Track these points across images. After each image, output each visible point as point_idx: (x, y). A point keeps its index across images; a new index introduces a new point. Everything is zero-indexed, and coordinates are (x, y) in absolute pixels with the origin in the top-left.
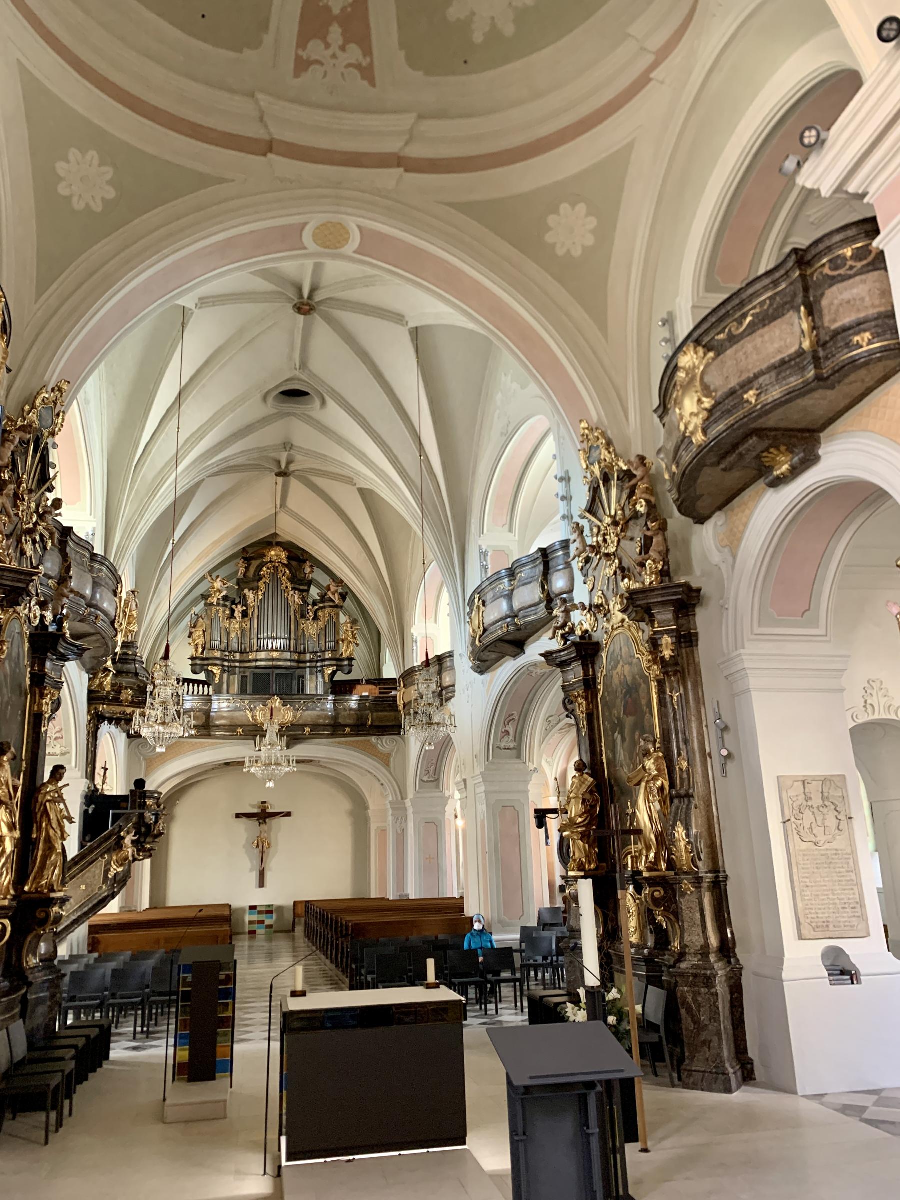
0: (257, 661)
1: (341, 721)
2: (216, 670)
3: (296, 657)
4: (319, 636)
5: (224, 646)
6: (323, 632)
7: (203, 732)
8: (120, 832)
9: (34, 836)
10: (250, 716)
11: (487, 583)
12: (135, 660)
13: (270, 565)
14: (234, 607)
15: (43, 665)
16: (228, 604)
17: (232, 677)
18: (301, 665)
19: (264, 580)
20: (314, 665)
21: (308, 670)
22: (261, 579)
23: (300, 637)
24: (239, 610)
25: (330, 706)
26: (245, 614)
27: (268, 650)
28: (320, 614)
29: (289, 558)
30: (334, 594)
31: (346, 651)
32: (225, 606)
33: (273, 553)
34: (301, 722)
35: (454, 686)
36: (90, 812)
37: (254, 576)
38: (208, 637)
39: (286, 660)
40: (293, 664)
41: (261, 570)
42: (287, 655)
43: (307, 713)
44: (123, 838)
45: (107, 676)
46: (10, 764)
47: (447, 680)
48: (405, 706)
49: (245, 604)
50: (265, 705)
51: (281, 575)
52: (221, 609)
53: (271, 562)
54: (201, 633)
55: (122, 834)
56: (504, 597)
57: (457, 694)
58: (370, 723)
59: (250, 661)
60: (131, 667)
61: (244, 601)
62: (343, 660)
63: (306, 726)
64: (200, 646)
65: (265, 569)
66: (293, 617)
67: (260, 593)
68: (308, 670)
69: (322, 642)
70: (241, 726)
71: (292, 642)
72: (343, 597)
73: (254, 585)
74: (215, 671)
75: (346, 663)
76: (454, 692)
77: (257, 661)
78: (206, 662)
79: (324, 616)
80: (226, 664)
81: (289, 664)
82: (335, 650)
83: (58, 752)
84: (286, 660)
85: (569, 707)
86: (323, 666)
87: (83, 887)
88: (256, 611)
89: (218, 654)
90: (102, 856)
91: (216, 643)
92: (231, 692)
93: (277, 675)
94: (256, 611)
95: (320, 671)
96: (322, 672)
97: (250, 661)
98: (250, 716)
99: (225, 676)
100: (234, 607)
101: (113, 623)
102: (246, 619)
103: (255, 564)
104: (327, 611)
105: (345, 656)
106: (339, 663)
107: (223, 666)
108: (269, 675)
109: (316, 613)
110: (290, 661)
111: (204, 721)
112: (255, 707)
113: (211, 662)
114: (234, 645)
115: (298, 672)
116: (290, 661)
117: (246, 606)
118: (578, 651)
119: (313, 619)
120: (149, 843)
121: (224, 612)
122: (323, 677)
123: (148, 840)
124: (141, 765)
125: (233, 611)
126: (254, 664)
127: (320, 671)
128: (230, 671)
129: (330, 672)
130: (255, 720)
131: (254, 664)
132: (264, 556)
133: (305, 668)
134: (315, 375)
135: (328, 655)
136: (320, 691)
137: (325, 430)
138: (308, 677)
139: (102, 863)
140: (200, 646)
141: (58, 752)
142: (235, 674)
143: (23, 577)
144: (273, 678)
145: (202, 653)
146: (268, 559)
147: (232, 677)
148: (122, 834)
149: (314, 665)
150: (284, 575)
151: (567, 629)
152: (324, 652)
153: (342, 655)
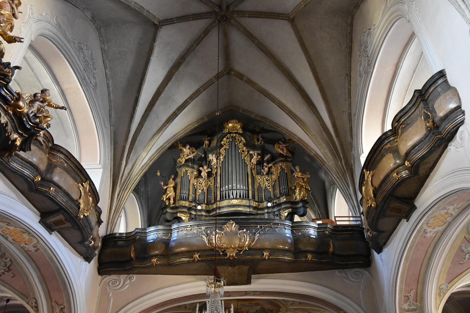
0: (220, 208)
1: (302, 247)
3: (254, 204)
4: (274, 187)
5: (190, 198)
6: (277, 183)
7: (164, 261)
13: (229, 135)
14: (201, 168)
18: (259, 212)
19: (224, 147)
20: (270, 210)
22: (221, 146)
25: (288, 233)
26: (209, 174)
28: (273, 170)
29: (243, 128)
31: (300, 194)
32: (193, 168)
33: (230, 125)
34: (258, 246)
38: (178, 191)
40: (251, 210)
41: (222, 140)
42: (245, 202)
49: (209, 166)
50: (221, 229)
51: (238, 142)
52: (190, 170)
53: (230, 133)
54: (172, 189)
58: (331, 250)
59: (214, 210)
62: (297, 203)
64: (172, 199)
66: (249, 173)
67: (221, 157)
69: (277, 191)
70: (198, 251)
74: (184, 218)
75: (300, 205)
77: (220, 208)
78: (175, 211)
80: (193, 213)
81: (248, 210)
86: (279, 210)
88: (219, 170)
89: (186, 204)
94: (219, 170)
100: (201, 168)
102: (211, 178)
106: (294, 206)
107: (191, 214)
109: (270, 168)
110: (249, 207)
111: (163, 249)
112: (212, 232)
113: (180, 210)
117: (212, 169)
119: (267, 174)
124: (109, 300)
125: (200, 172)
127: (277, 215)
129: (286, 214)
130: (211, 244)
135: (283, 199)
140: (172, 199)
146: (226, 131)
149: (270, 210)
150: (240, 142)
153: (296, 199)
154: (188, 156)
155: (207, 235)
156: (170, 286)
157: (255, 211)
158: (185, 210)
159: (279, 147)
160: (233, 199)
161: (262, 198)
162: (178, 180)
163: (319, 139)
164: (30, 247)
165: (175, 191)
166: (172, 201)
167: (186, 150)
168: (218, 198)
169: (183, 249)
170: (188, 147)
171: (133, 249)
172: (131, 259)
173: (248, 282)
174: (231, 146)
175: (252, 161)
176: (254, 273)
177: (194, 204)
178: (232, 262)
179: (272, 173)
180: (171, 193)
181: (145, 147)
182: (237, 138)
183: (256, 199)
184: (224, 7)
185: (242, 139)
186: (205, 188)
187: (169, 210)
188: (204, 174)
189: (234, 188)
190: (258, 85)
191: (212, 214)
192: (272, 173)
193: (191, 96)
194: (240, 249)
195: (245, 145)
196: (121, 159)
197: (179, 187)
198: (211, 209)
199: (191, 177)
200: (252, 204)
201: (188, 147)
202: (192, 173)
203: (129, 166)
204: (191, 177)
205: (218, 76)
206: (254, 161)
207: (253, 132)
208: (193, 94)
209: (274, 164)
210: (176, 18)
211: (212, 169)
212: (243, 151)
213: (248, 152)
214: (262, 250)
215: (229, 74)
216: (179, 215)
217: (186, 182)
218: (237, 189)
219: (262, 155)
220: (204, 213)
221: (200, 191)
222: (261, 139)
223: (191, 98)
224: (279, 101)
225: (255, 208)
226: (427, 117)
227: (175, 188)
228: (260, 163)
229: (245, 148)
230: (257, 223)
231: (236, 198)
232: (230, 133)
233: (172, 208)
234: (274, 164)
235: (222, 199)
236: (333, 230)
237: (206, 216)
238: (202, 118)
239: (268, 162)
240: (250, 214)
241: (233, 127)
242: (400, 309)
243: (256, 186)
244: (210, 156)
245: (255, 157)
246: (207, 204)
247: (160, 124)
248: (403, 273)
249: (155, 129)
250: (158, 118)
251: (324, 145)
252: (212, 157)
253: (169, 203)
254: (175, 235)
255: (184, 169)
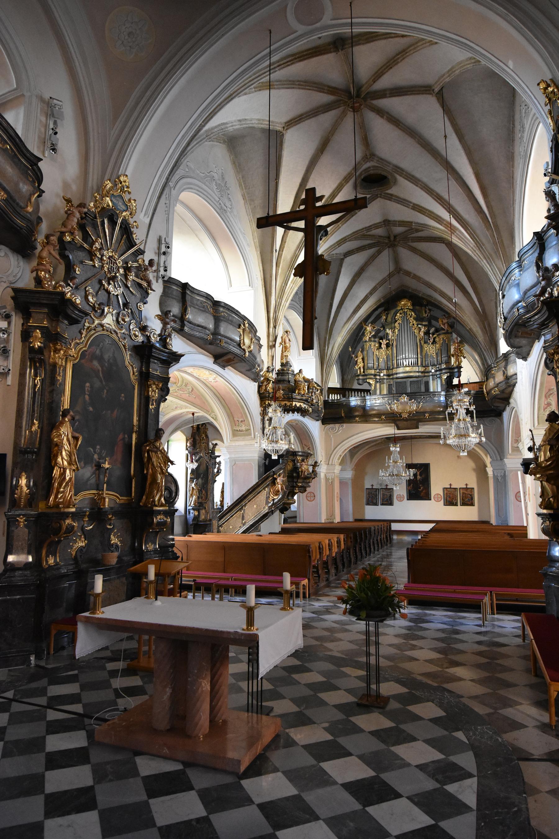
0: (397, 374)
2: (371, 382)
3: (421, 369)
4: (437, 354)
6: (439, 352)
8: (274, 475)
9: (145, 472)
10: (388, 408)
11: (504, 278)
12: (288, 373)
13: (401, 311)
14: (381, 341)
15: (148, 367)
16: (377, 340)
17: (382, 385)
18: (426, 374)
21: (431, 377)
22: (396, 321)
23: (425, 356)
24: (384, 342)
25: (442, 399)
26: (388, 345)
27: (403, 367)
28: (437, 339)
29: (413, 305)
30: (444, 324)
32: (375, 341)
33: (403, 303)
34: (422, 410)
35: (516, 374)
36: (267, 463)
37: (392, 319)
38: (366, 362)
39: (415, 372)
40: (420, 374)
42: (416, 369)
43: (425, 404)
44: (276, 479)
45: (269, 383)
46: (70, 423)
47: (511, 371)
48: (488, 395)
50: (398, 401)
51: (409, 317)
52: (373, 344)
53: (402, 309)
55: (275, 476)
56: (514, 286)
57: (518, 380)
59: (393, 375)
60: (286, 378)
61: (386, 336)
62: (454, 368)
63: (426, 412)
65: (398, 314)
66: (418, 344)
67: (396, 331)
68: (431, 377)
69: (439, 358)
70: (384, 414)
71: (419, 360)
72: (451, 326)
73: (393, 325)
74: (371, 382)
75: (456, 370)
76: (517, 379)
77: (397, 374)
78: (365, 377)
79: (440, 340)
80: (378, 377)
81: (417, 374)
82: (448, 362)
83: (244, 429)
84: (415, 372)
85: (550, 365)
86: (440, 374)
87: (255, 506)
89: (373, 372)
90: (264, 489)
91: (371, 365)
92: (382, 393)
93: (410, 381)
95: (439, 377)
96: (440, 377)
97: (393, 375)
98: (388, 408)
99: (378, 385)
100: (381, 341)
101: (239, 345)
102: (389, 348)
103: (393, 312)
104: (441, 337)
105: (455, 365)
106: (451, 371)
107: (376, 379)
108: (406, 382)
109: (434, 339)
110: (418, 372)
111: (362, 412)
113: (368, 377)
114: (382, 365)
115: (425, 379)
116: (418, 372)
117: (389, 340)
118: (549, 309)
119: (432, 343)
120: (300, 483)
121: (375, 345)
122: (441, 380)
123: (299, 481)
124: (331, 440)
125: (380, 344)
126: (395, 376)
128: (381, 381)
129: (445, 377)
131: (395, 376)
132: (396, 306)
133: (429, 376)
134: (381, 159)
135: (444, 366)
136: (439, 390)
137: (404, 202)
138: (431, 382)
139: (264, 493)
141: (244, 429)
142: (384, 383)
143: (54, 297)
144: (408, 384)
145: (364, 372)
147: (382, 385)
148: (275, 476)
150: (411, 317)
151: (547, 295)
152: (440, 364)
154: (371, 333)
155: (389, 404)
156: (367, 431)
157: (423, 375)
158: (372, 377)
159: (442, 321)
160: (406, 366)
161: (428, 364)
162: (365, 353)
163: (472, 319)
164: (294, 424)
165: (364, 362)
166: (362, 370)
167: (369, 329)
168: (395, 366)
169: (374, 412)
170: (370, 325)
171: (343, 412)
172: (342, 417)
173: (417, 428)
174: (403, 321)
175: (421, 333)
176: (421, 422)
177: (378, 371)
178: (406, 420)
179: (436, 343)
180: (361, 365)
181: (339, 334)
182: (408, 313)
183: (424, 365)
184: (392, 238)
185: (413, 313)
186: (385, 357)
187: (361, 377)
188: (384, 346)
189: (407, 357)
190: (423, 279)
191: (391, 377)
192: (436, 343)
193: (370, 292)
194: (410, 413)
195: (414, 319)
196: (325, 346)
197: (366, 358)
198: (391, 373)
199: (374, 349)
200: (420, 370)
201: (370, 325)
202: (375, 345)
203: (330, 349)
204: (374, 349)
205: (390, 275)
206: (422, 334)
207: (421, 305)
208: (371, 290)
209: (438, 335)
210: (356, 249)
211: (389, 340)
212: (413, 325)
213: (417, 325)
214: (424, 413)
215: (399, 273)
216: (368, 381)
217: (371, 354)
218: (409, 358)
219: (430, 326)
220: (385, 377)
221: (381, 360)
222: (428, 311)
223: (371, 293)
224: (441, 291)
225: (422, 372)
226: (504, 373)
227: (363, 359)
228: (427, 333)
229: (414, 322)
230: (421, 395)
231: (409, 366)
232: (402, 309)
233: (363, 376)
234: (438, 335)
235: (398, 367)
236: (475, 394)
237: (387, 379)
238: (379, 300)
239: (433, 334)
240: (419, 377)
241: (404, 305)
242: (512, 447)
243: (424, 354)
244: (387, 330)
245: (423, 330)
246: (388, 369)
247: (349, 315)
248: (513, 428)
249: (345, 320)
250: (346, 310)
251: (476, 324)
252: (389, 331)
253: (360, 371)
254: (368, 403)
255: (368, 344)
